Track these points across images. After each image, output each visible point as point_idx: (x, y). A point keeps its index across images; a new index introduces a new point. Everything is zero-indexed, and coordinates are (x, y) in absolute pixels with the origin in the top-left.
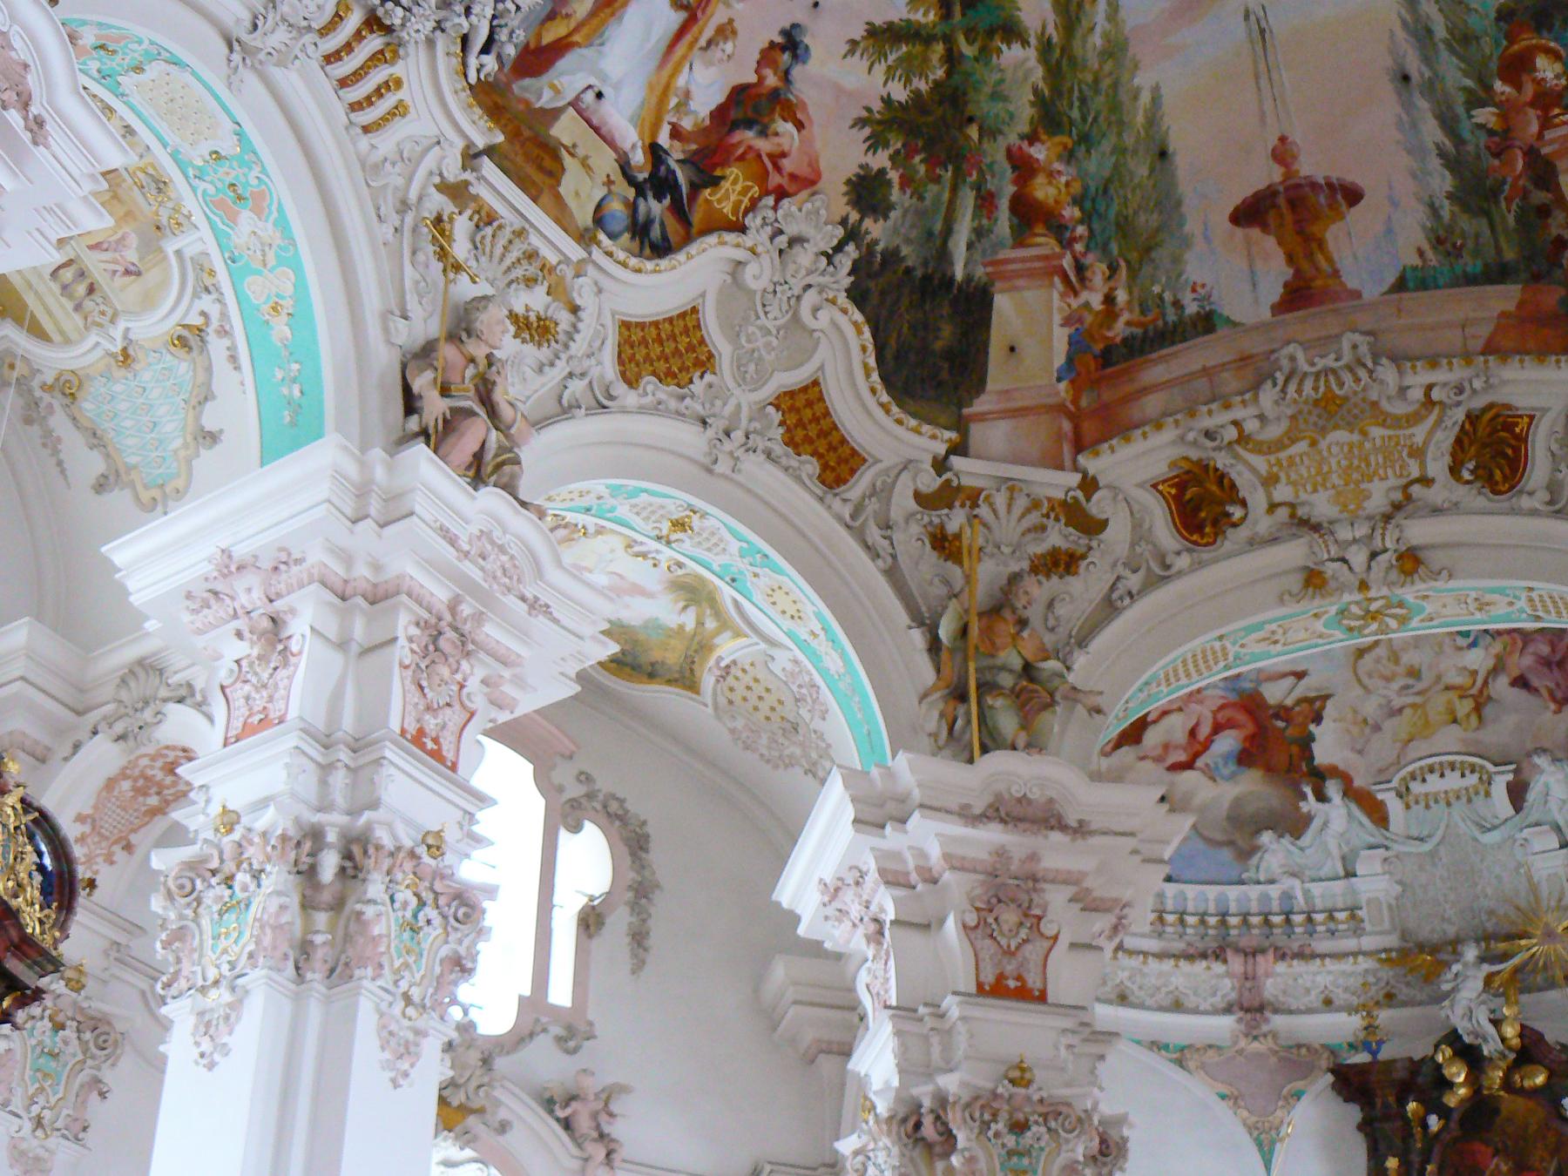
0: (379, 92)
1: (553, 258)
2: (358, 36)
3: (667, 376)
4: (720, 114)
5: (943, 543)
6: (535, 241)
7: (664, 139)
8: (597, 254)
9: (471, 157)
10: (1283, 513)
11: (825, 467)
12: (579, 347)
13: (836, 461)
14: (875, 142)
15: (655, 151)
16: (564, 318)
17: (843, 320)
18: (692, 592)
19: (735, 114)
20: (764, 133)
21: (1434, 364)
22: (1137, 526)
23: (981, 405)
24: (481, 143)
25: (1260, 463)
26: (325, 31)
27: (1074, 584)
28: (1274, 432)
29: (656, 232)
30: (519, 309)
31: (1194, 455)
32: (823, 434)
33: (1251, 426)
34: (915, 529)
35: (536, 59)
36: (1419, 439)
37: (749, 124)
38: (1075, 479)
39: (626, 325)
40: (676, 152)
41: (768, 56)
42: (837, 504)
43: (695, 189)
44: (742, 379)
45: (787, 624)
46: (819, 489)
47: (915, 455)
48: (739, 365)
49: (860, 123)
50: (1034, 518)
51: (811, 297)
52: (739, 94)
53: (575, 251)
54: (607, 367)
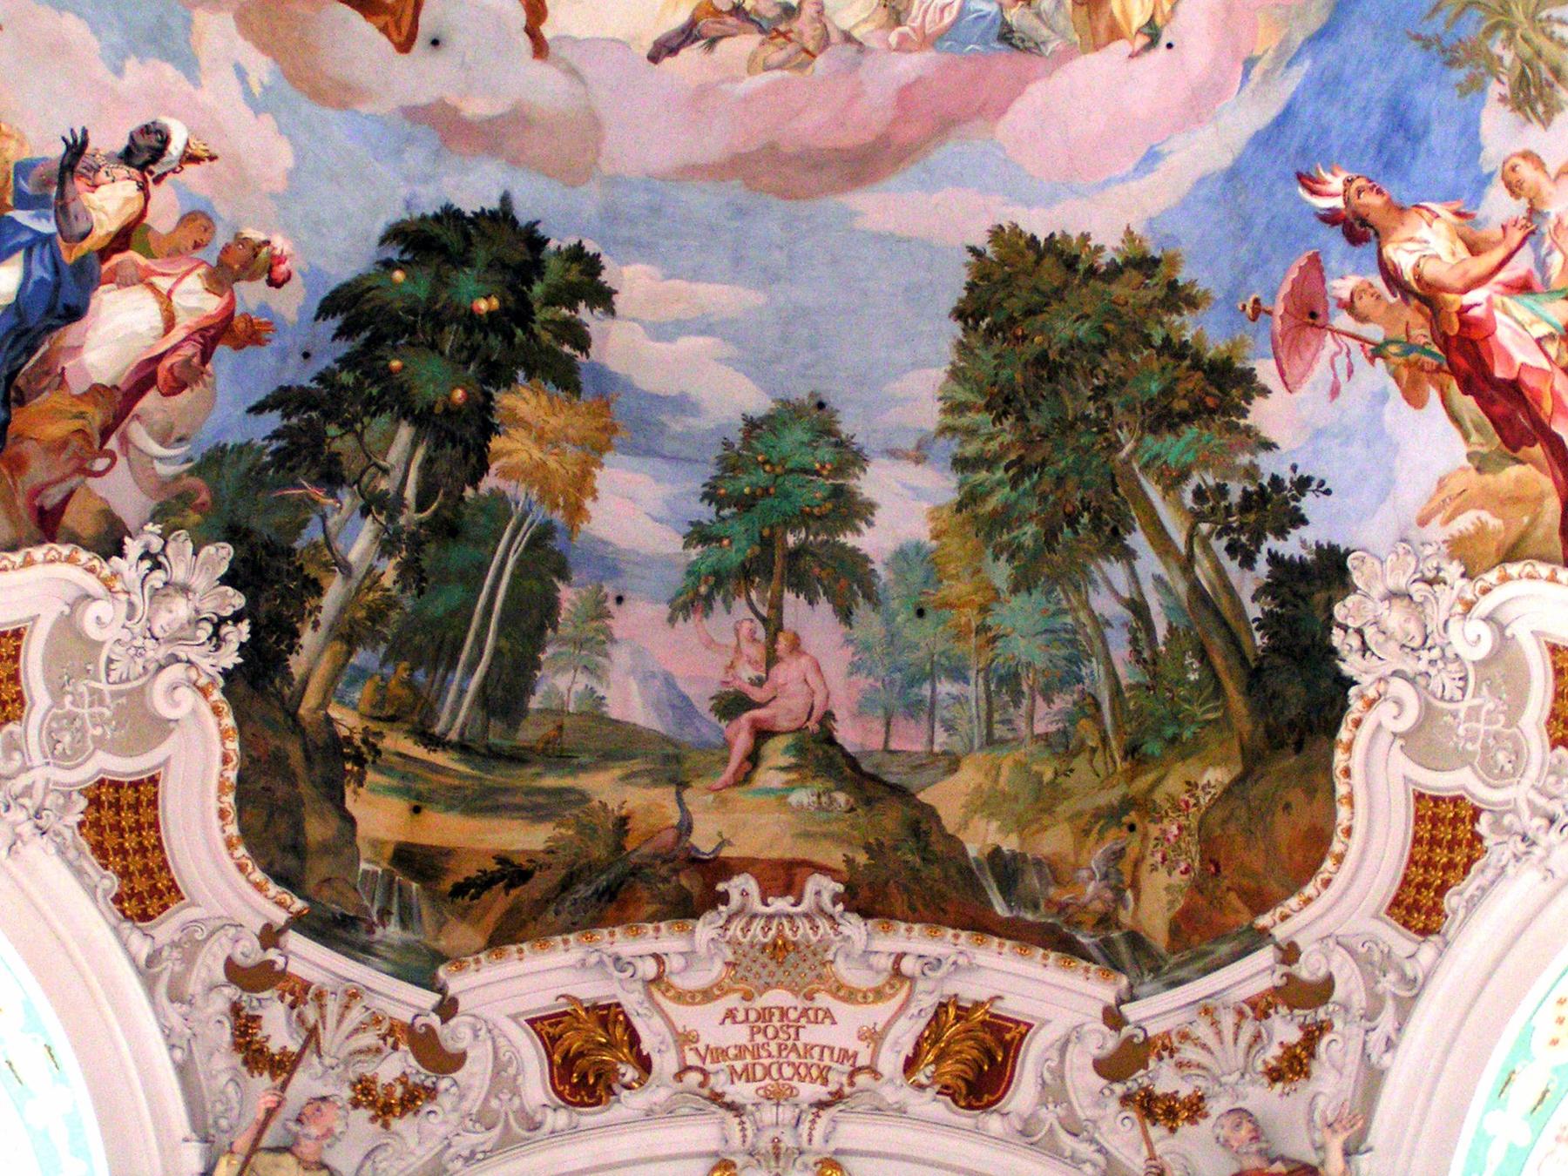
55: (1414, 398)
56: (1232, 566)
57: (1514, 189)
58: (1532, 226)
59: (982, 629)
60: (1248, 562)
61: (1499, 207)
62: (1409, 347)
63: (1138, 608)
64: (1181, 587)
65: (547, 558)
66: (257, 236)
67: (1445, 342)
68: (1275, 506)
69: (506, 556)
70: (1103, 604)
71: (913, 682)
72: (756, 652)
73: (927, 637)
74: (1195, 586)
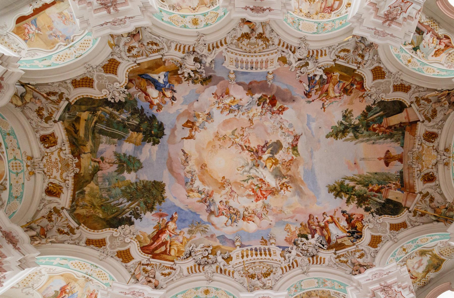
0: (321, 260)
1: (354, 250)
2: (313, 259)
3: (379, 243)
4: (348, 223)
5: (422, 215)
6: (350, 251)
7: (347, 231)
8: (357, 244)
9: (335, 254)
10: (433, 167)
11: (403, 227)
12: (367, 251)
13: (404, 225)
14: (361, 207)
15: (348, 232)
16: (363, 252)
17: (383, 218)
18: (423, 253)
19: (349, 221)
20: (353, 219)
21: (414, 144)
22: (430, 188)
23: (403, 204)
24: (334, 251)
25: (424, 169)
26: (310, 262)
27: (436, 198)
28: (420, 166)
29: (359, 236)
30: (358, 257)
31: (421, 178)
32: (398, 226)
33: (418, 169)
34: (418, 218)
35: (329, 241)
36: (427, 147)
37: (351, 220)
38: (419, 195)
39: (369, 245)
40: (350, 230)
41: (344, 215)
42: (409, 227)
43: (356, 229)
44: (385, 233)
45: (429, 241)
46: (406, 229)
47: (406, 215)
48: (383, 233)
49: (358, 207)
50: (423, 202)
51: (378, 221)
52: (347, 220)
53: (355, 246)
54: (373, 249)
55: (154, 228)
56: (129, 213)
57: (180, 232)
58: (176, 235)
59: (116, 187)
60: (130, 214)
61: (178, 231)
62: (160, 226)
63: (121, 203)
64: (125, 208)
65: (121, 138)
66: (163, 109)
67: (162, 229)
68: (138, 216)
69: (121, 133)
70: (121, 200)
71: (108, 179)
72: (110, 161)
73: (114, 181)
74: (125, 209)
